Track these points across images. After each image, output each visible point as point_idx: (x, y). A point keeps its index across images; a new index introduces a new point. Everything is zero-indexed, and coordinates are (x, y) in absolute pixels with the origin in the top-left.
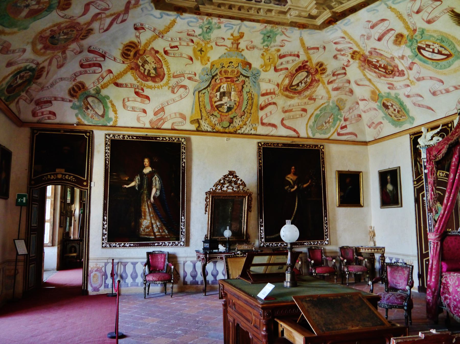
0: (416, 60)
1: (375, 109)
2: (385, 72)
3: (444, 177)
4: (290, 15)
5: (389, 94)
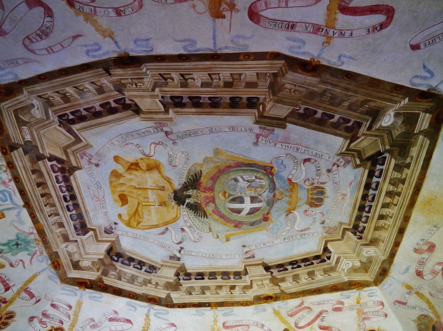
4: (66, 247)
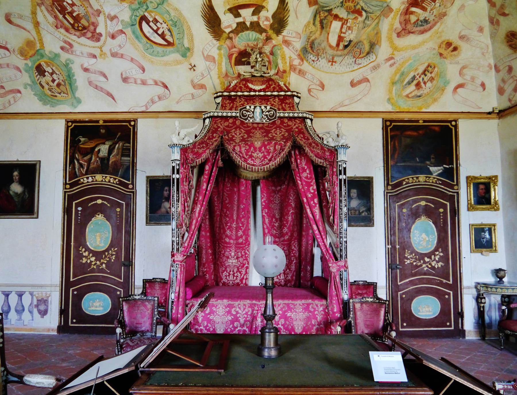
0: (128, 31)
1: (18, 69)
2: (73, 26)
3: (116, 184)
5: (57, 55)
